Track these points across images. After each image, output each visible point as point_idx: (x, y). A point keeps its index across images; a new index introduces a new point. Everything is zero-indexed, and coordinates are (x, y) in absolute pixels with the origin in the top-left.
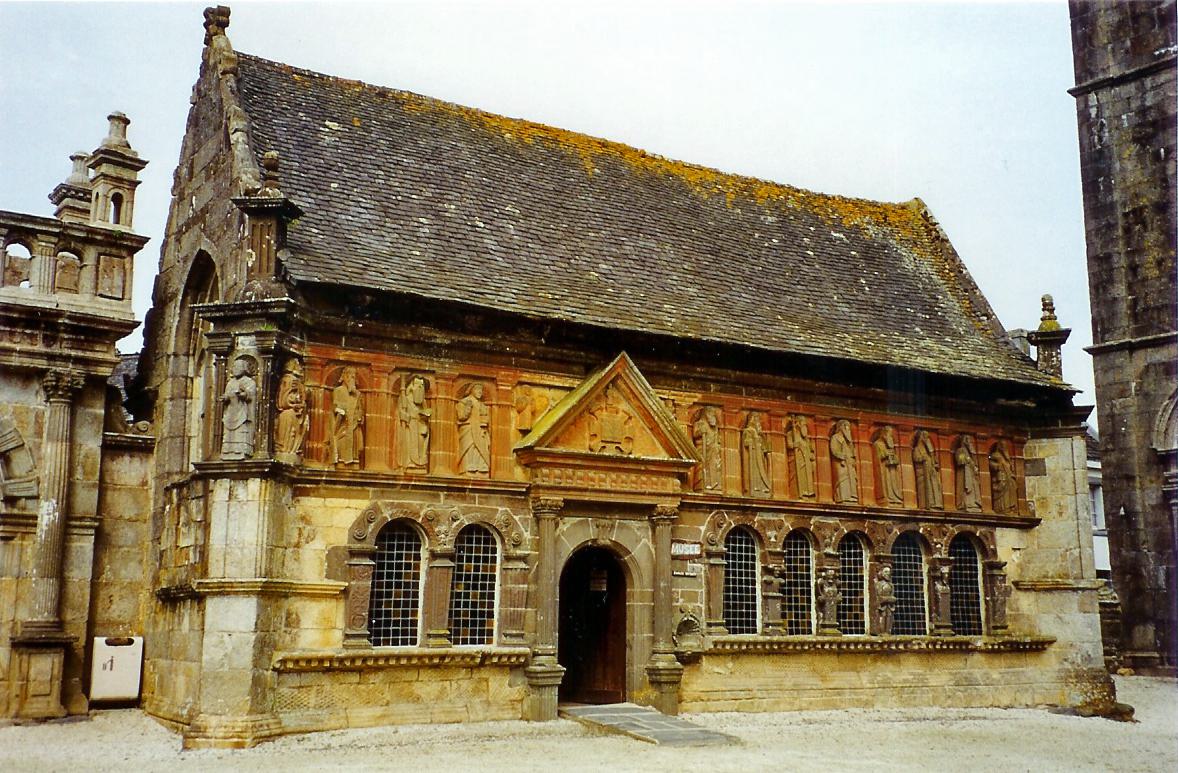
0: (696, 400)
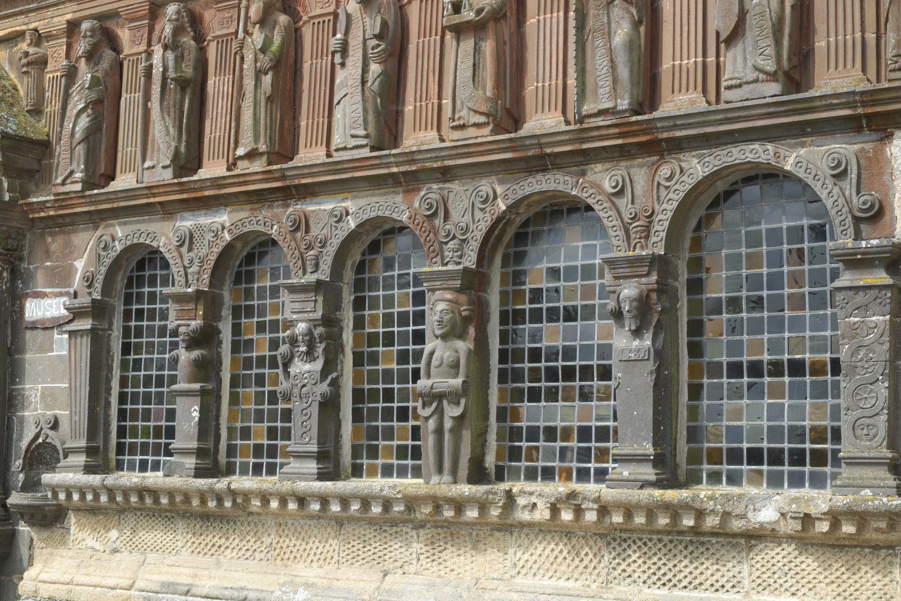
0: (69, 17)
